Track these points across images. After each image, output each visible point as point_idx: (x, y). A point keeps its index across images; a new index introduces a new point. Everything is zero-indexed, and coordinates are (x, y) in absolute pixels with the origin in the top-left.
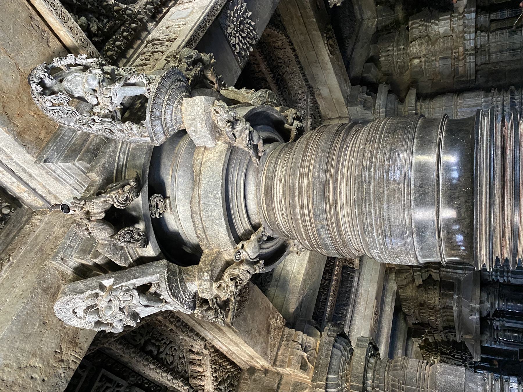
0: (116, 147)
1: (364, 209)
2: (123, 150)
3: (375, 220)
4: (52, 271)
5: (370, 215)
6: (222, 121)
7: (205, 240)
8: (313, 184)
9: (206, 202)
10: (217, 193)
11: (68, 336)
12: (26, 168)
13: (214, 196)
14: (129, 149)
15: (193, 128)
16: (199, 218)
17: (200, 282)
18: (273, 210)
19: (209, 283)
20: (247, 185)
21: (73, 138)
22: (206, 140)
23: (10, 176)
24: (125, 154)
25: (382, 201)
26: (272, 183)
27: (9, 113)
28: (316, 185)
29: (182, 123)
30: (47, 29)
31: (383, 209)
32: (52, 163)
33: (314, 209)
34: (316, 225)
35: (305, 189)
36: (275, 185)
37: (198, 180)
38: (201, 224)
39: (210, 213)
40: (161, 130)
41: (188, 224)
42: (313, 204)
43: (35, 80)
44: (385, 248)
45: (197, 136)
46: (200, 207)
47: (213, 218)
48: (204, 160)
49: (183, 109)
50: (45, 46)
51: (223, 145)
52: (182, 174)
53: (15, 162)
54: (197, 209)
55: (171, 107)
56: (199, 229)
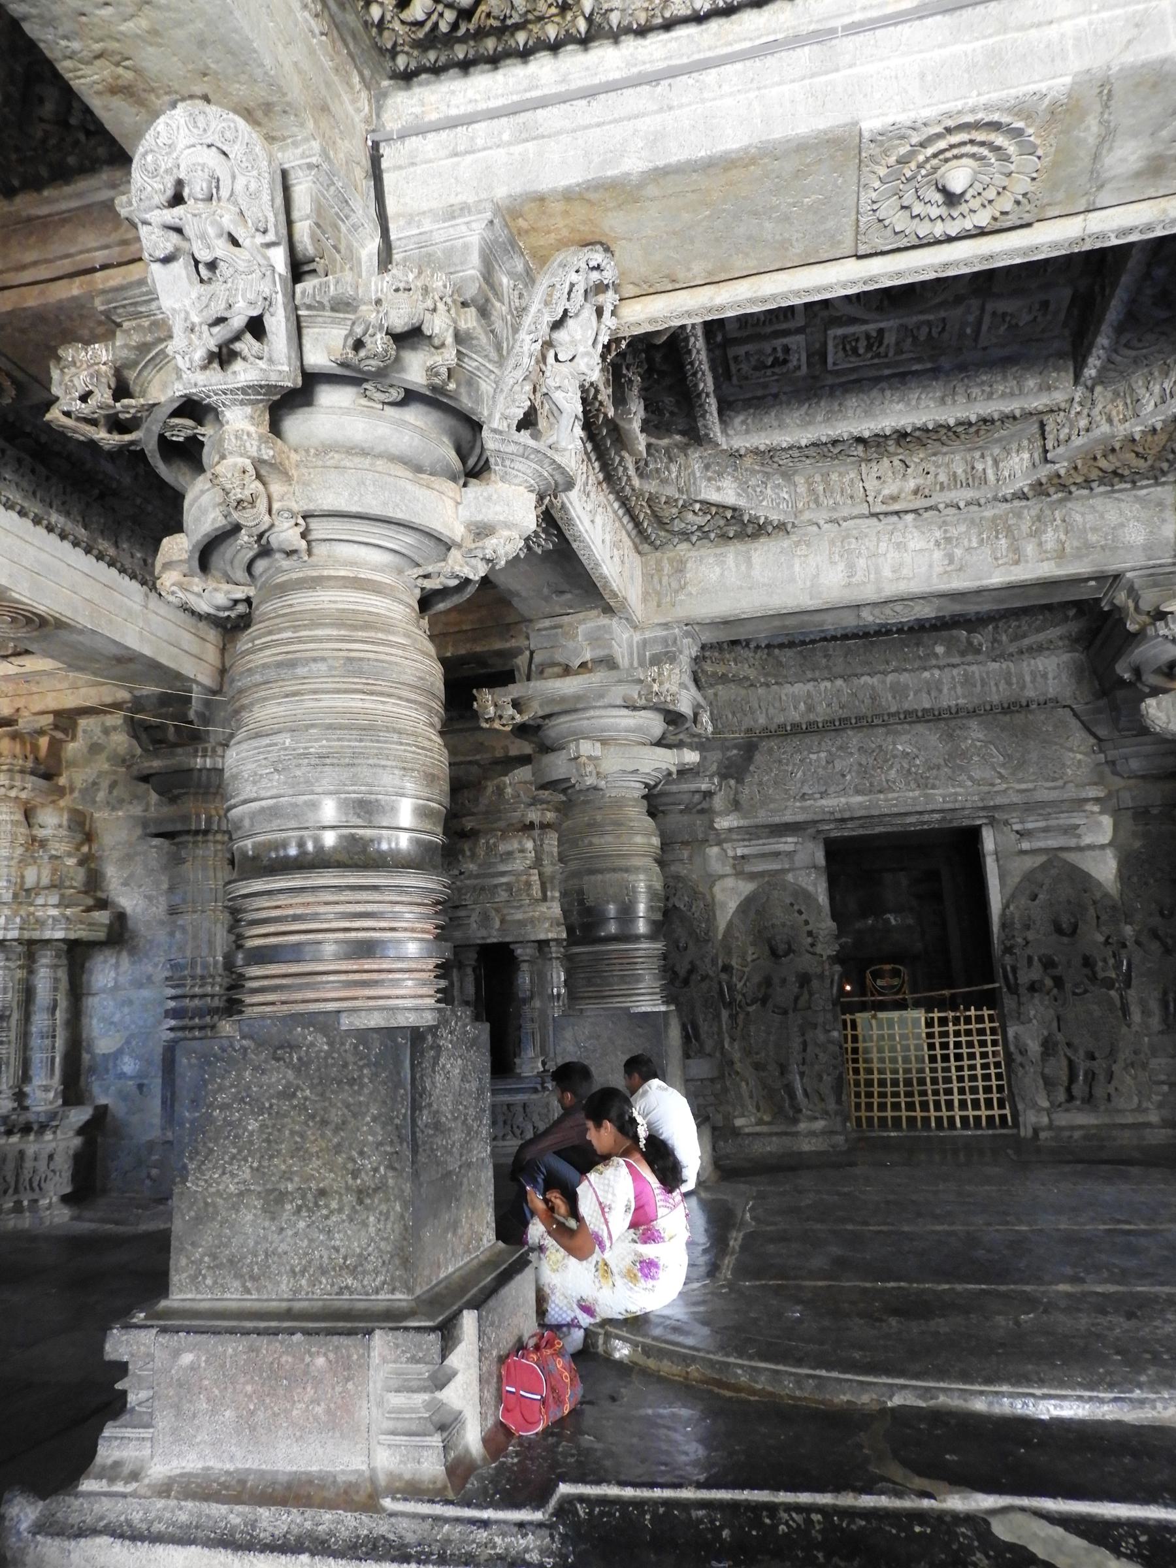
0: (490, 361)
7: (320, 463)
15: (495, 497)
29: (503, 479)
33: (361, 659)
34: (334, 658)
49: (522, 489)
54: (380, 469)
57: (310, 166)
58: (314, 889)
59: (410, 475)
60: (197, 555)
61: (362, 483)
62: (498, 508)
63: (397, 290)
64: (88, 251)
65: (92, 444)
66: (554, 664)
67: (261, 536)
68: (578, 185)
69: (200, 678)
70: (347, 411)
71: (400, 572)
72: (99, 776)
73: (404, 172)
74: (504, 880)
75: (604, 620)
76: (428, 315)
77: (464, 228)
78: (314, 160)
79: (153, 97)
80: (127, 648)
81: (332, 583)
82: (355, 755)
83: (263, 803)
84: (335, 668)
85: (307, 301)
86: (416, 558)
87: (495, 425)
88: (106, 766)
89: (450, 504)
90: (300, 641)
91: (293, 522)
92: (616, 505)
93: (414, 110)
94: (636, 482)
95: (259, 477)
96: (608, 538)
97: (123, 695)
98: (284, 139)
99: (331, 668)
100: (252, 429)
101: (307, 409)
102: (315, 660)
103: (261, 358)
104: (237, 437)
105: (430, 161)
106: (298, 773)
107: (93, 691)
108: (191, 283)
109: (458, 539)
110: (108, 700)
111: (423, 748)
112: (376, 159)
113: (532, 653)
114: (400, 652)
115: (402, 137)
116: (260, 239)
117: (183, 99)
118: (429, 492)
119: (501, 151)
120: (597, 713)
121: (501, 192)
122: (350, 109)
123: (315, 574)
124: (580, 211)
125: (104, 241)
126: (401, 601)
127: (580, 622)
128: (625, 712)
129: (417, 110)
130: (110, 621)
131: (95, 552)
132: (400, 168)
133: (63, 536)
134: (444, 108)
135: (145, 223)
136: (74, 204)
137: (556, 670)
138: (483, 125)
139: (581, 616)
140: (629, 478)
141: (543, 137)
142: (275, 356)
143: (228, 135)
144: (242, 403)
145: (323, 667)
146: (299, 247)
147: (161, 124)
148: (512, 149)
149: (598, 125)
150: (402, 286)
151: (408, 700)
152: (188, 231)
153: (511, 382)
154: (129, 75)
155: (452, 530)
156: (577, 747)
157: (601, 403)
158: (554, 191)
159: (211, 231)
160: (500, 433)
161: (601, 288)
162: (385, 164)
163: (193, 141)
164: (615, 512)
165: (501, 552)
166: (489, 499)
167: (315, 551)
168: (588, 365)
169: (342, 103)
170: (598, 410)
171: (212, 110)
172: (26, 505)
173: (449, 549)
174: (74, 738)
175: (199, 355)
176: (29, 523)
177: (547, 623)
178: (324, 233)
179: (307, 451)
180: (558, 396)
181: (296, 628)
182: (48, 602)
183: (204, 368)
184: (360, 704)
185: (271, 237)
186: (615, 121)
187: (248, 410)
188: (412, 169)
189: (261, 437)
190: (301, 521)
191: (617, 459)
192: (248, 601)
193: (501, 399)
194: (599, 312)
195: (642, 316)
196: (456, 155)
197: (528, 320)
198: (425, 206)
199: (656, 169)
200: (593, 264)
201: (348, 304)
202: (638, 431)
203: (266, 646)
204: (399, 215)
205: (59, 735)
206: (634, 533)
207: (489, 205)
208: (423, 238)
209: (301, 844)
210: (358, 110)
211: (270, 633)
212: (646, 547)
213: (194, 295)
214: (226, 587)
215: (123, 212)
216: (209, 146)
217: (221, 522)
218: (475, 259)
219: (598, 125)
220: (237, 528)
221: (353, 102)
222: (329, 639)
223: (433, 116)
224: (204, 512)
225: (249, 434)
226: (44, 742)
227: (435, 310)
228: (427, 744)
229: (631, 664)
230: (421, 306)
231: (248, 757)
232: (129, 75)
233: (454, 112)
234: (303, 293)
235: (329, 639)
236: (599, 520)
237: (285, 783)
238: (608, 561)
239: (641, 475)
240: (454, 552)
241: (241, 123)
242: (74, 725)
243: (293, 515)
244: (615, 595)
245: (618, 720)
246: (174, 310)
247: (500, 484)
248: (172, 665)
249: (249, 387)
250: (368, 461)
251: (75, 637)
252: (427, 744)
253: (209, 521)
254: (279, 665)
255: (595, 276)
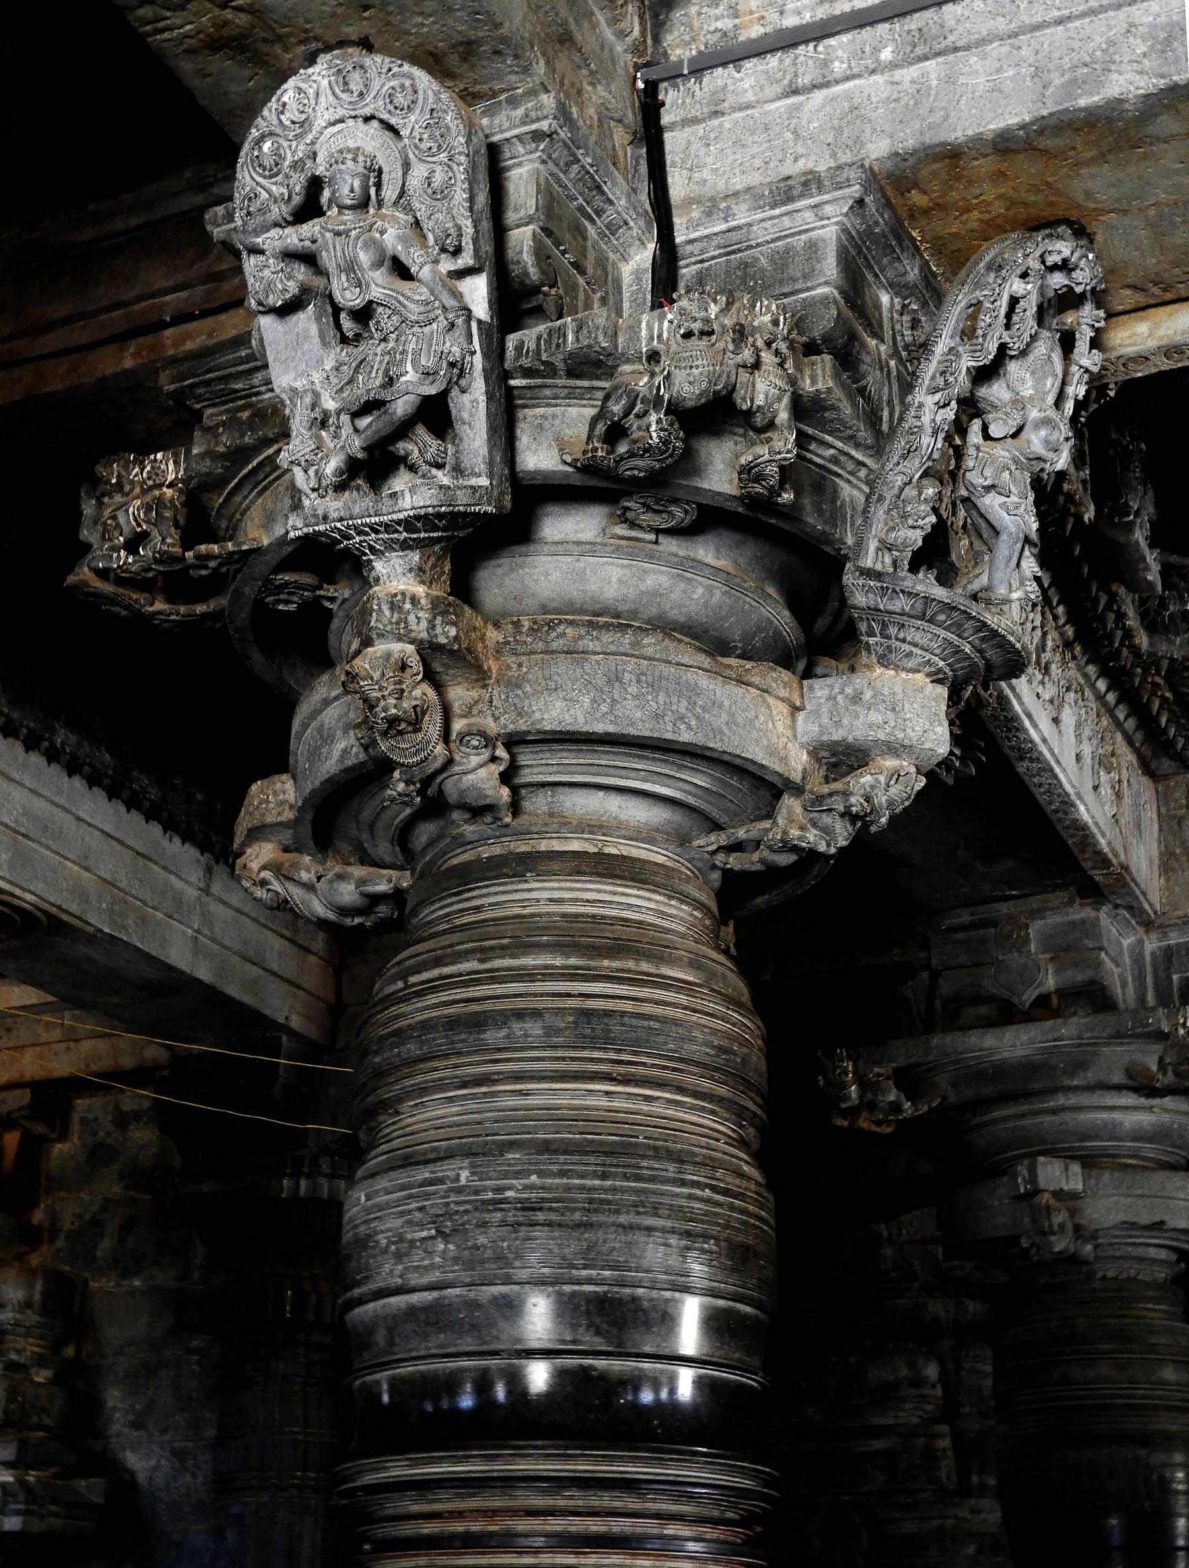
0: (857, 446)
1: (615, 1161)
2: (842, 458)
3: (582, 1188)
4: (513, 78)
5: (595, 1175)
6: (873, 787)
7: (540, 646)
8: (675, 1022)
9: (664, 683)
10: (689, 727)
11: (265, 40)
12: (824, 92)
13: (682, 718)
14: (839, 475)
15: (868, 695)
16: (621, 649)
17: (423, 601)
18: (579, 873)
19: (424, 635)
20: (650, 800)
21: (876, 276)
22: (825, 720)
23: (807, 17)
24: (830, 461)
25: (638, 1213)
26: (657, 887)
27: (1021, 156)
28: (674, 1031)
29: (884, 662)
30: (1168, 296)
31: (617, 1212)
32: (846, 215)
33: (608, 1014)
34: (559, 1011)
35: (659, 994)
36: (648, 895)
37: (728, 672)
38: (598, 649)
39: (633, 689)
40: (890, 607)
41: (556, 576)
42: (623, 1014)
43: (1076, 255)
44: (483, 1202)
45: (839, 697)
46: (650, 659)
47: (616, 696)
48: (771, 700)
49: (919, 677)
50: (1129, 281)
51: (800, 768)
52: (714, 601)
53: (859, 76)
54: (649, 652)
55: (937, 651)
56: (581, 637)
57: (537, 136)
58: (508, 1482)
59: (705, 661)
60: (309, 816)
61: (615, 679)
62: (875, 717)
63: (688, 335)
64: (153, 295)
65: (142, 620)
66: (979, 999)
67: (427, 781)
68: (1023, 126)
69: (295, 1022)
70: (589, 548)
71: (682, 840)
72: (103, 1209)
73: (700, 129)
74: (878, 1445)
75: (1081, 912)
76: (744, 376)
77: (809, 215)
78: (544, 125)
79: (278, 50)
80: (170, 968)
81: (555, 866)
82: (594, 1205)
83: (415, 1298)
84: (558, 1031)
85: (525, 362)
86: (715, 813)
87: (868, 562)
88: (117, 1189)
89: (780, 709)
90: (494, 977)
91: (486, 754)
92: (1102, 685)
93: (719, 25)
94: (1143, 640)
95: (430, 676)
96: (1087, 749)
97: (154, 1050)
98: (494, 94)
99: (550, 1031)
100: (420, 590)
101: (516, 549)
102: (520, 1015)
103: (440, 466)
104: (393, 607)
105: (749, 106)
106: (482, 1240)
107: (102, 1046)
108: (325, 344)
109: (796, 777)
110: (128, 1062)
111: (726, 1192)
112: (650, 107)
113: (935, 975)
114: (682, 999)
115: (699, 68)
116: (447, 265)
117: (328, 49)
118: (740, 691)
119: (877, 78)
120: (1073, 1100)
121: (878, 149)
122: (609, 34)
123: (523, 848)
124: (1027, 170)
125: (179, 278)
126: (684, 898)
127: (1035, 914)
128: (1129, 1099)
129: (726, 24)
130: (144, 920)
131: (126, 794)
132: (695, 121)
133: (72, 769)
134: (772, 15)
135: (256, 251)
136: (134, 221)
137: (984, 1010)
138: (845, 38)
139: (1034, 902)
140: (1128, 634)
141: (956, 49)
142: (466, 463)
143: (400, 99)
144: (405, 546)
145: (535, 1029)
146: (515, 271)
147: (288, 92)
148: (898, 74)
149: (1060, 22)
150: (696, 326)
151: (696, 1095)
152: (328, 260)
153: (899, 481)
154: (242, 19)
155: (784, 760)
156: (1033, 1170)
157: (1070, 497)
158: (977, 140)
159: (364, 258)
160: (878, 576)
161: (1068, 300)
162: (666, 119)
163: (341, 112)
164: (1100, 698)
165: (881, 799)
166: (856, 699)
167: (526, 805)
168: (1047, 442)
169: (594, 26)
170: (1065, 511)
171: (374, 62)
172: (15, 715)
173: (777, 795)
174: (63, 1136)
175: (331, 467)
176: (19, 748)
177: (965, 917)
178: (557, 244)
179: (517, 625)
180: (991, 503)
181: (485, 954)
182: (39, 887)
183: (340, 487)
184: (604, 1102)
185: (466, 259)
186: (1092, 12)
187: (415, 557)
188: (715, 122)
189: (435, 603)
190: (501, 752)
191: (1103, 600)
192: (397, 896)
193: (879, 513)
194: (1067, 342)
195: (1152, 344)
196: (796, 92)
197: (930, 369)
198: (738, 183)
199: (1173, 88)
200: (1051, 260)
201: (598, 364)
202: (1143, 544)
203: (431, 988)
204: (689, 201)
205: (40, 1129)
206: (1138, 737)
207: (853, 174)
208: (735, 236)
209: (483, 1386)
210: (622, 35)
211: (438, 962)
212: (1166, 765)
213: (329, 365)
214: (358, 871)
215: (217, 232)
216: (367, 119)
217: (357, 755)
218: (830, 267)
219: (1060, 22)
220: (382, 768)
221: (614, 21)
222: (548, 974)
223: (756, 31)
224: (327, 738)
225: (414, 600)
226: (12, 1139)
227: (757, 365)
228: (733, 1182)
229: (1142, 999)
230: (732, 361)
231: (388, 1206)
232: (242, 19)
233: (791, 21)
234: (519, 348)
235: (548, 974)
236: (1068, 717)
237: (456, 1260)
238: (1089, 796)
239: (1152, 625)
240: (790, 805)
241: (422, 78)
242: (69, 1108)
243: (489, 741)
244: (1104, 862)
245: (1117, 1116)
246: (294, 391)
247: (879, 670)
248: (247, 999)
249: (418, 518)
250: (627, 639)
251: (82, 949)
252: (733, 1182)
253: (336, 754)
254: (453, 1023)
255: (1058, 280)
